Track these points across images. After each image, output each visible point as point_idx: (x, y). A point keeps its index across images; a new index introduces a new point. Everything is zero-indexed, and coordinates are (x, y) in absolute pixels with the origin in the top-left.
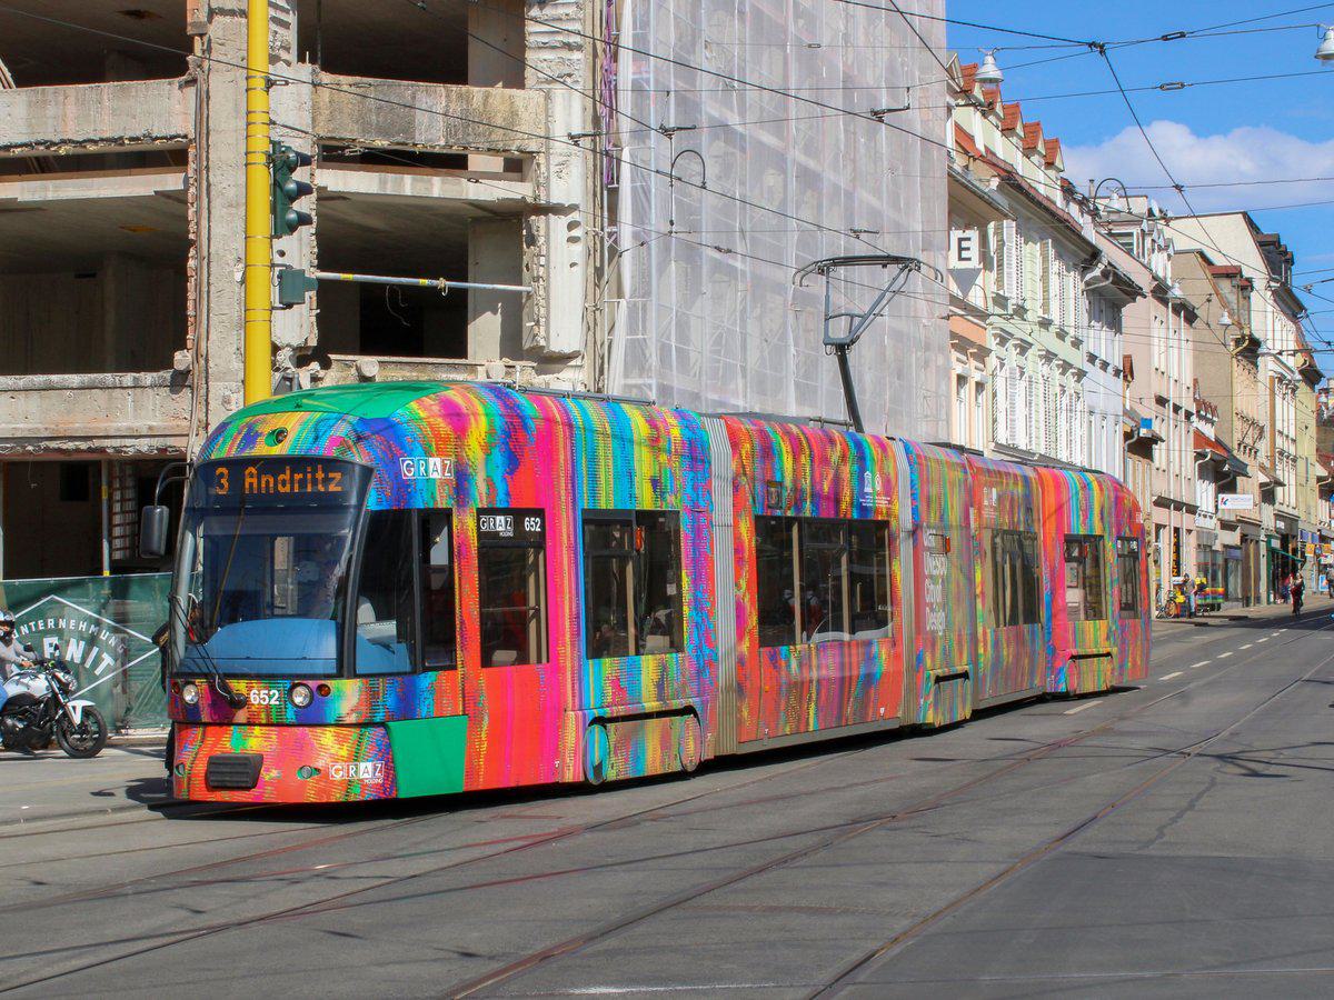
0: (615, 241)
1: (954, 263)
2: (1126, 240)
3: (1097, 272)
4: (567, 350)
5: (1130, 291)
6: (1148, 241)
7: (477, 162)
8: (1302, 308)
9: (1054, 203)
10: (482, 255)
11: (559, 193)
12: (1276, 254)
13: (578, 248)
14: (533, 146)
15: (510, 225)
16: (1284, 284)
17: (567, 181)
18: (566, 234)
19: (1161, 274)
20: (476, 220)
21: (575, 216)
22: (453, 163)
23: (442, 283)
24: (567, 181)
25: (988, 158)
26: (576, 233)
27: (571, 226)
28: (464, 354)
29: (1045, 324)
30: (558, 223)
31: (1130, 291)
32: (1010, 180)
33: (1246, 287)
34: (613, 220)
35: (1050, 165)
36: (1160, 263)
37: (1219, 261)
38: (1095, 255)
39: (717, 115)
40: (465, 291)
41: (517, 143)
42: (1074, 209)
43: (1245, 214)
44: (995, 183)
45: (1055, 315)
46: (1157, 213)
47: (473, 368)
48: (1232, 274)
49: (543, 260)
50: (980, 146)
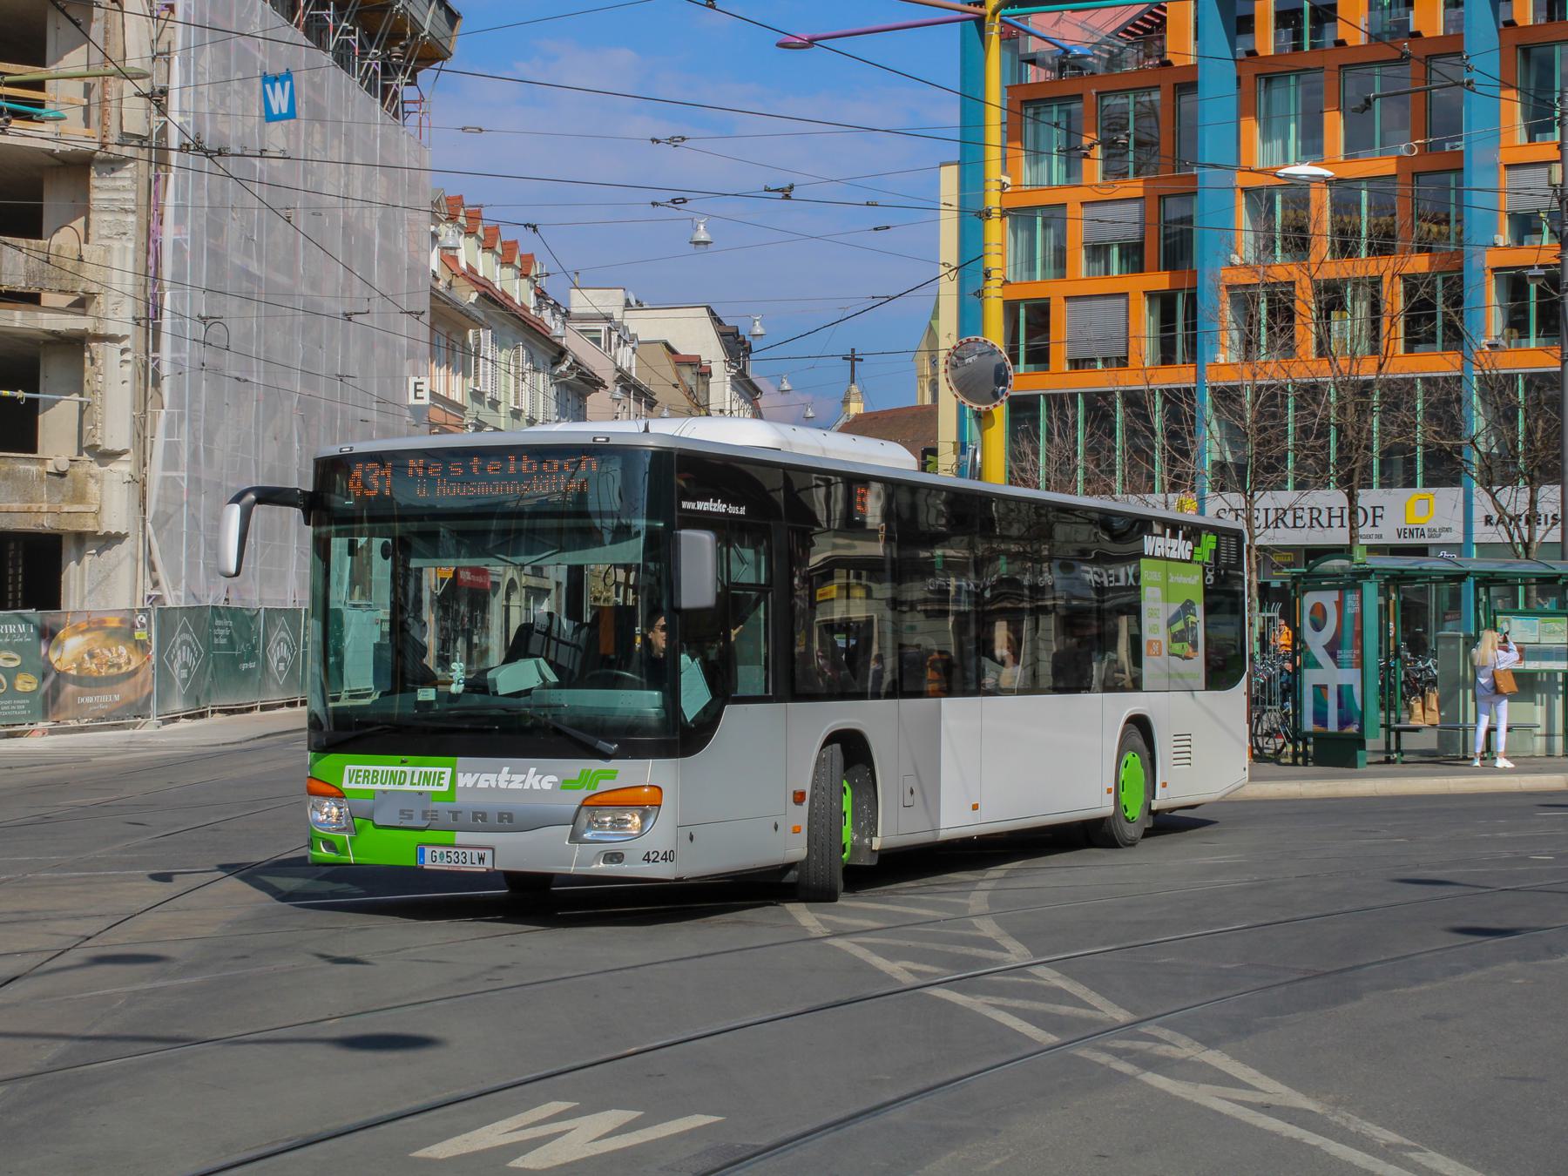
0: (158, 365)
1: (412, 401)
2: (595, 335)
3: (563, 368)
4: (118, 449)
5: (596, 384)
6: (614, 336)
7: (47, 299)
8: (757, 390)
9: (527, 310)
10: (51, 370)
11: (112, 328)
12: (736, 344)
13: (128, 368)
14: (94, 289)
15: (74, 346)
16: (742, 373)
17: (117, 313)
18: (119, 358)
19: (625, 367)
20: (47, 342)
21: (124, 345)
22: (31, 299)
23: (20, 394)
24: (117, 313)
25: (471, 275)
26: (128, 356)
27: (123, 351)
28: (34, 450)
29: (516, 414)
30: (113, 350)
31: (596, 384)
32: (491, 298)
33: (704, 374)
34: (156, 349)
35: (525, 276)
36: (625, 357)
37: (682, 351)
38: (562, 353)
39: (238, 262)
40: (37, 400)
41: (83, 285)
42: (546, 314)
43: (708, 308)
44: (474, 297)
45: (526, 406)
46: (633, 303)
47: (43, 461)
48: (693, 362)
49: (100, 378)
50: (463, 265)
